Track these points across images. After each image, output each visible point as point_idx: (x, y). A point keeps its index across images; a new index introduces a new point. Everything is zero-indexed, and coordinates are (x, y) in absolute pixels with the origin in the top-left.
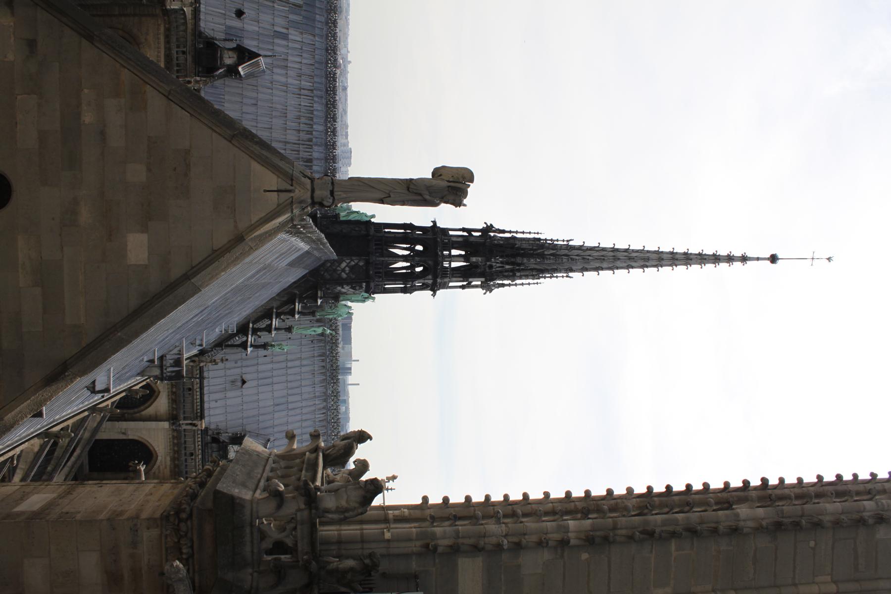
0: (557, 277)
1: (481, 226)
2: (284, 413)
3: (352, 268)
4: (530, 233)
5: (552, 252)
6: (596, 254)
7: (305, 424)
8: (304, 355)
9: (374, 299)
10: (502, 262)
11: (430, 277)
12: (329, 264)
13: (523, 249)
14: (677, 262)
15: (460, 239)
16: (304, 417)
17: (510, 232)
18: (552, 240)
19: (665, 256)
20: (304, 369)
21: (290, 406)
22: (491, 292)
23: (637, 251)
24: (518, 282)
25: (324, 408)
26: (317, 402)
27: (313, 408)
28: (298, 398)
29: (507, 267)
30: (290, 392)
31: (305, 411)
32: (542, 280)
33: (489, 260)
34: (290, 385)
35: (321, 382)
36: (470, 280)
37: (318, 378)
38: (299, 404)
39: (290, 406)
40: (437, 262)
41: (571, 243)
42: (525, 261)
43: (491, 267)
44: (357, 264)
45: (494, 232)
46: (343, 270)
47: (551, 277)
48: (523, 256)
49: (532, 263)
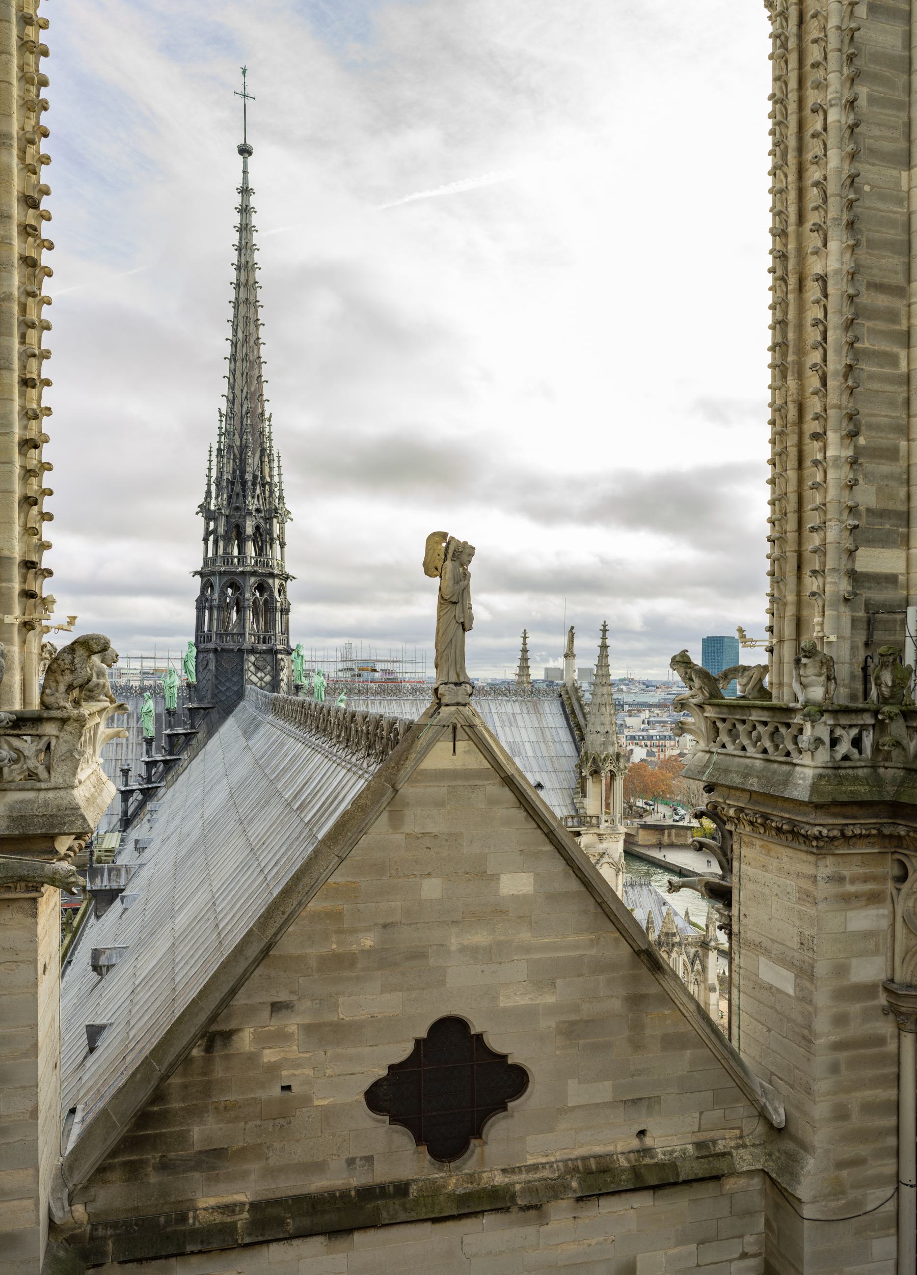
0: (270, 433)
1: (200, 520)
3: (258, 669)
4: (210, 461)
5: (237, 436)
6: (239, 381)
9: (298, 646)
10: (253, 498)
11: (270, 581)
13: (234, 471)
14: (251, 282)
15: (221, 544)
17: (209, 485)
18: (220, 435)
19: (242, 296)
22: (289, 512)
23: (235, 331)
24: (276, 479)
29: (258, 491)
32: (275, 452)
33: (250, 513)
36: (275, 536)
40: (254, 573)
41: (224, 412)
42: (249, 469)
43: (258, 510)
44: (254, 664)
45: (209, 503)
46: (261, 679)
47: (271, 440)
48: (243, 472)
49: (253, 462)
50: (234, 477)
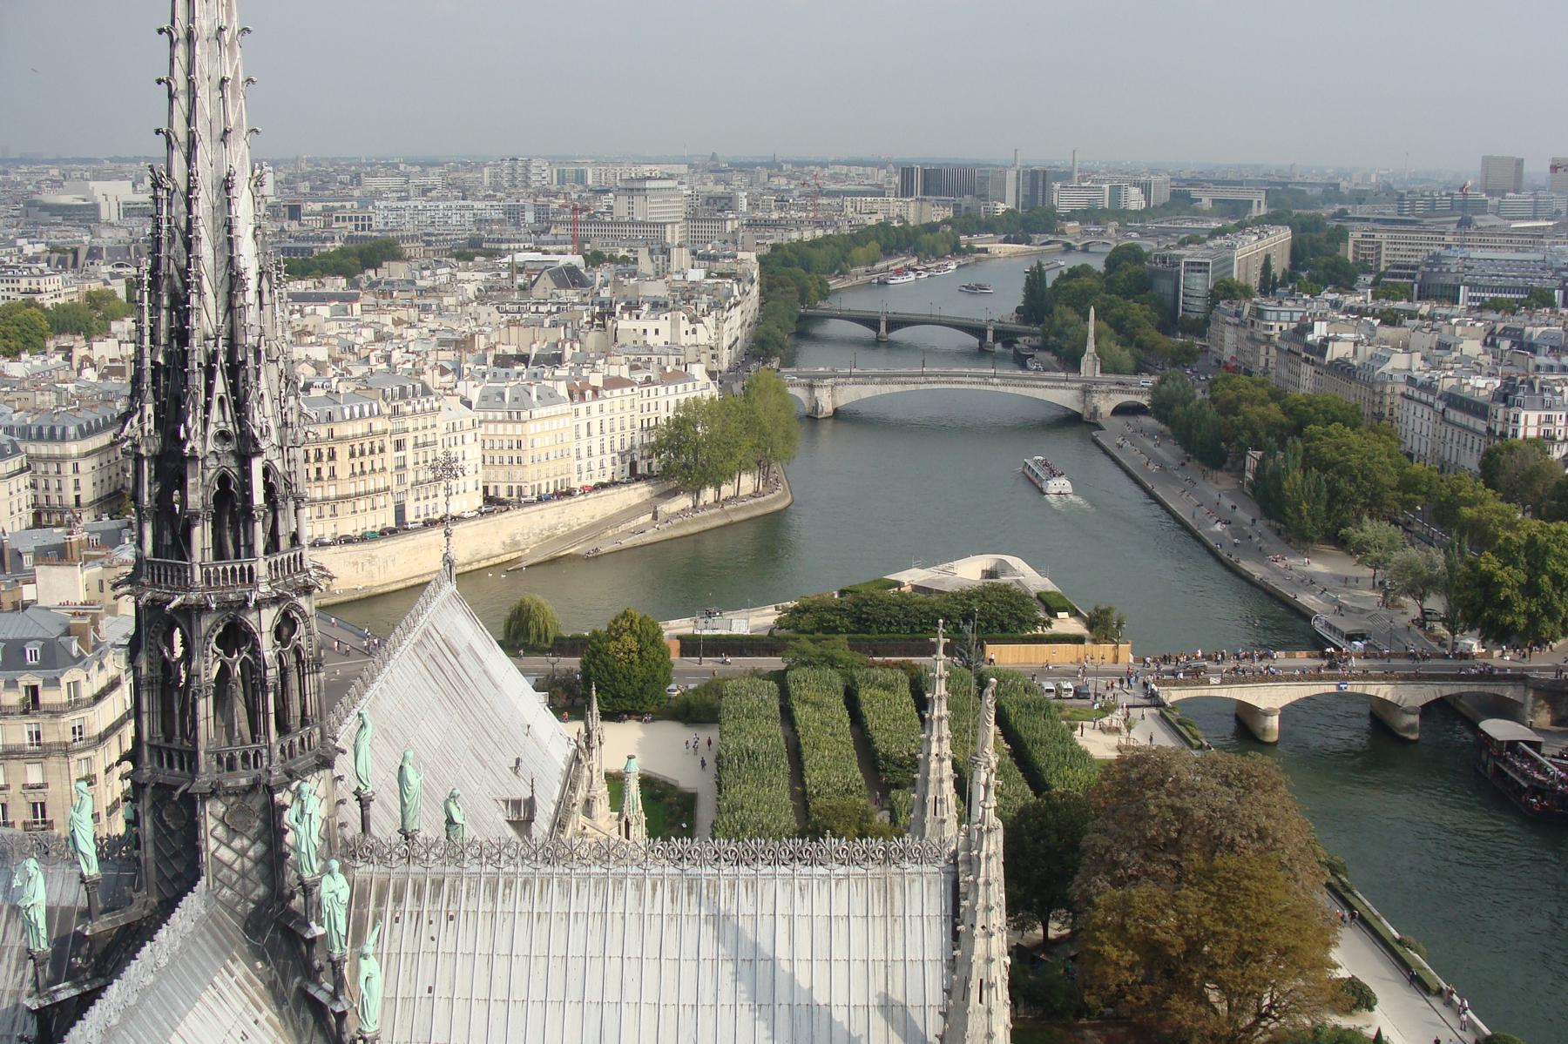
2: (629, 1013)
3: (233, 832)
7: (670, 951)
8: (483, 947)
12: (226, 892)
16: (652, 950)
20: (521, 946)
21: (612, 995)
25: (639, 887)
27: (632, 922)
28: (595, 967)
29: (220, 387)
30: (575, 994)
31: (633, 950)
34: (556, 993)
39: (612, 995)
44: (222, 821)
46: (242, 853)
50: (167, 356)
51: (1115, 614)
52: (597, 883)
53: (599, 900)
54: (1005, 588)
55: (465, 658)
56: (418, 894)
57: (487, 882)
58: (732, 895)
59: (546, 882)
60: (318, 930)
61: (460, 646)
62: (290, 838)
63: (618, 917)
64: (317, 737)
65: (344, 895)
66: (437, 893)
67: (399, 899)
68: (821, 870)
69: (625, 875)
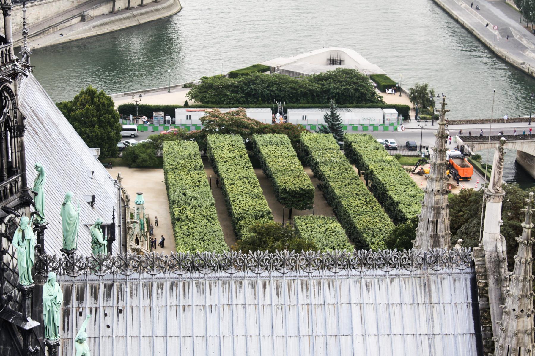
7: (279, 330)
8: (145, 331)
16: (266, 331)
20: (173, 330)
25: (253, 286)
26: (240, 301)
27: (251, 310)
35: (202, 292)
37: (195, 297)
38: (242, 339)
51: (429, 89)
52: (224, 284)
53: (226, 295)
54: (349, 73)
55: (46, 123)
56: (95, 295)
57: (145, 285)
58: (320, 289)
59: (186, 285)
60: (31, 324)
61: (43, 116)
62: (6, 258)
63: (240, 307)
64: (20, 184)
65: (61, 298)
66: (108, 295)
67: (81, 298)
68: (379, 272)
69: (243, 278)
